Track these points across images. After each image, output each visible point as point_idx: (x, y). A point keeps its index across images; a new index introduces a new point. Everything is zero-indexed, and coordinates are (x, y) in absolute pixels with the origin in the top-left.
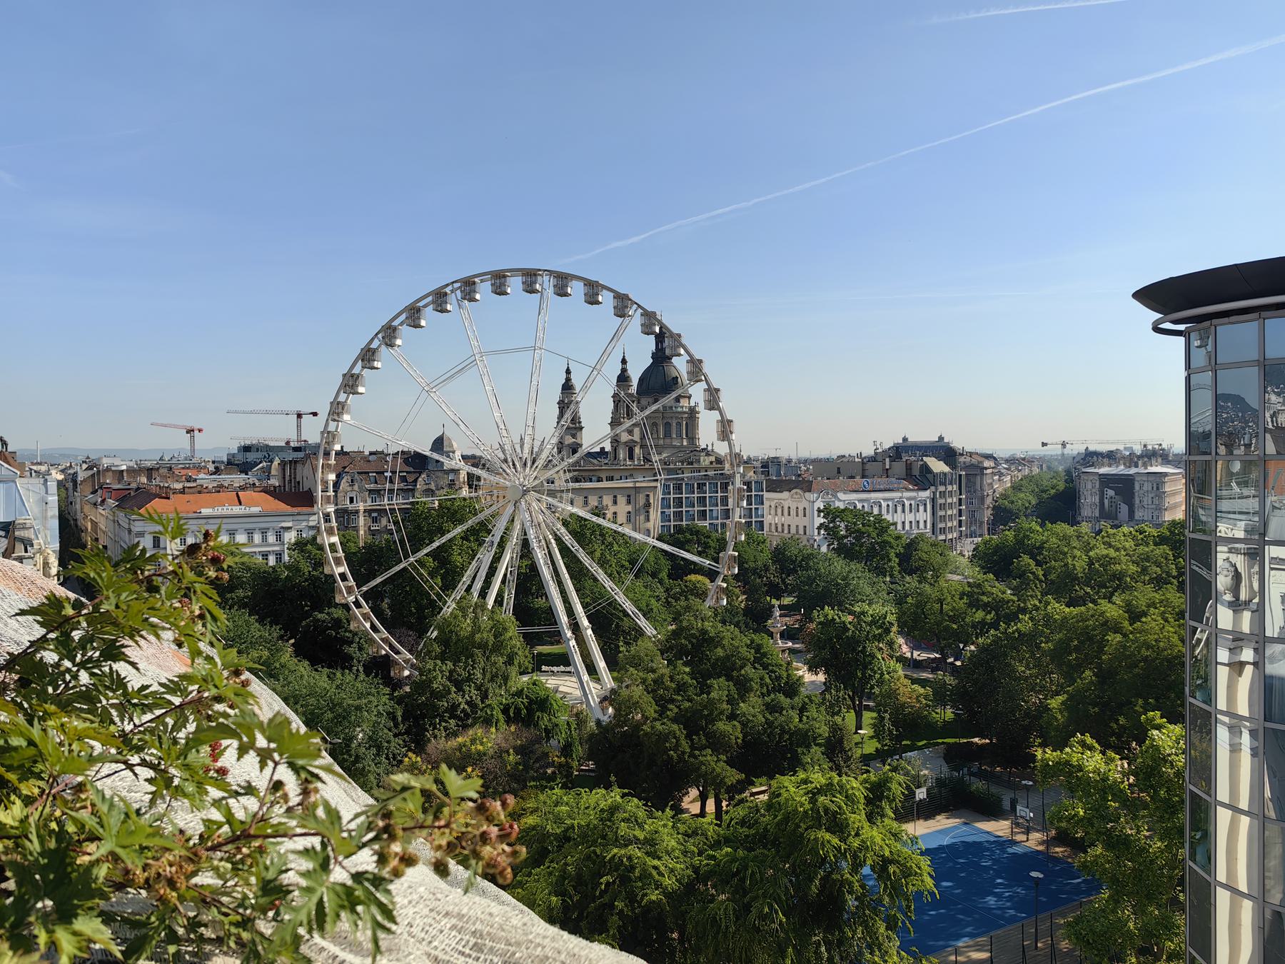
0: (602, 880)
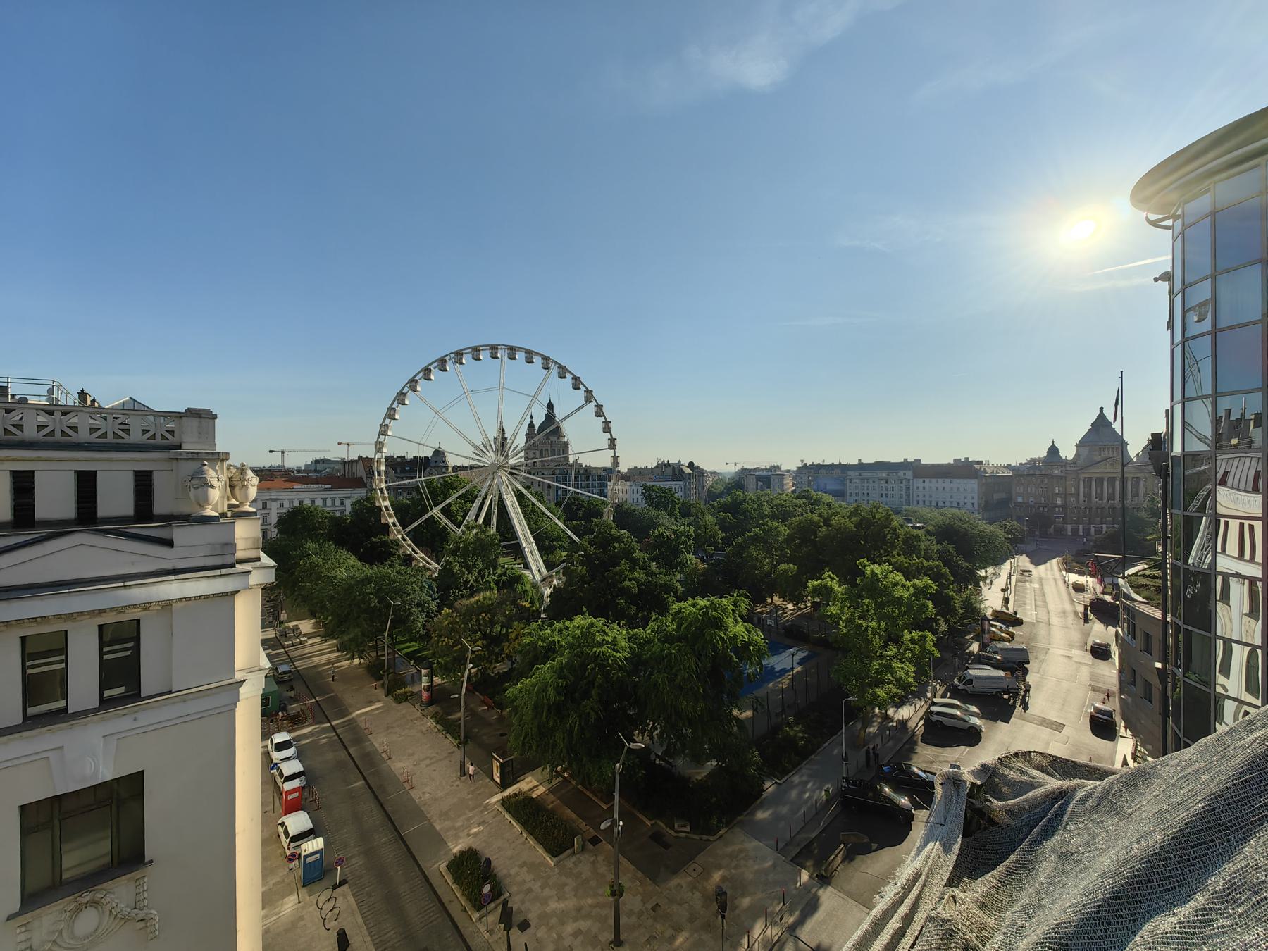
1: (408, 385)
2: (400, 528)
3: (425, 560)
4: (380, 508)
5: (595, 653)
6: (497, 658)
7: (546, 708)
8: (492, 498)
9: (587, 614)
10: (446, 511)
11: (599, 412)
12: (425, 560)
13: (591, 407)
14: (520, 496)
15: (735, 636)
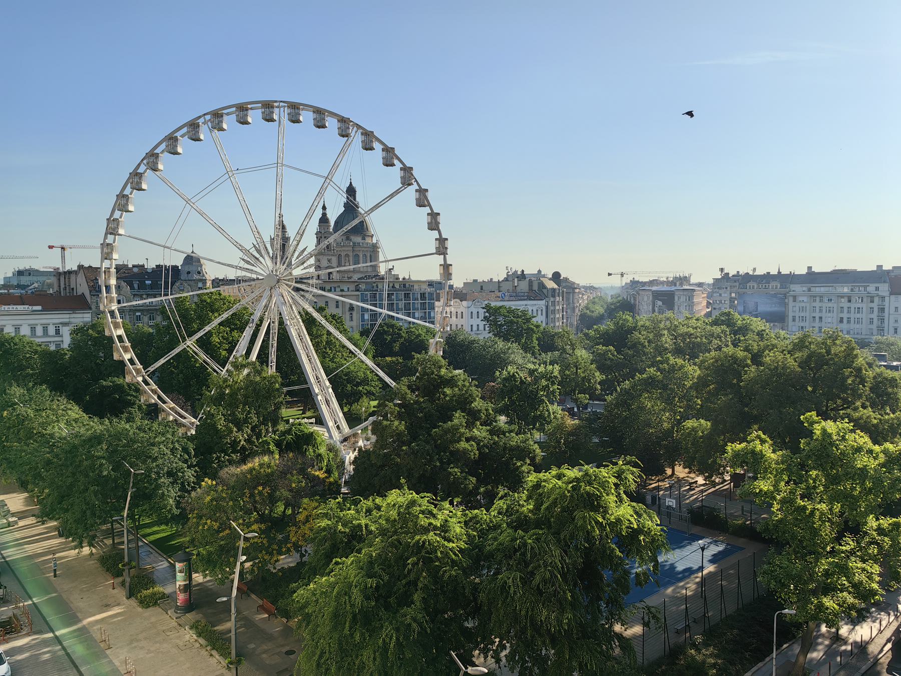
0: (409, 562)
1: (145, 162)
2: (140, 366)
3: (177, 412)
4: (110, 339)
5: (418, 541)
6: (280, 548)
7: (350, 616)
8: (269, 324)
9: (406, 488)
10: (204, 343)
11: (422, 200)
12: (177, 412)
13: (410, 193)
14: (309, 322)
15: (619, 521)
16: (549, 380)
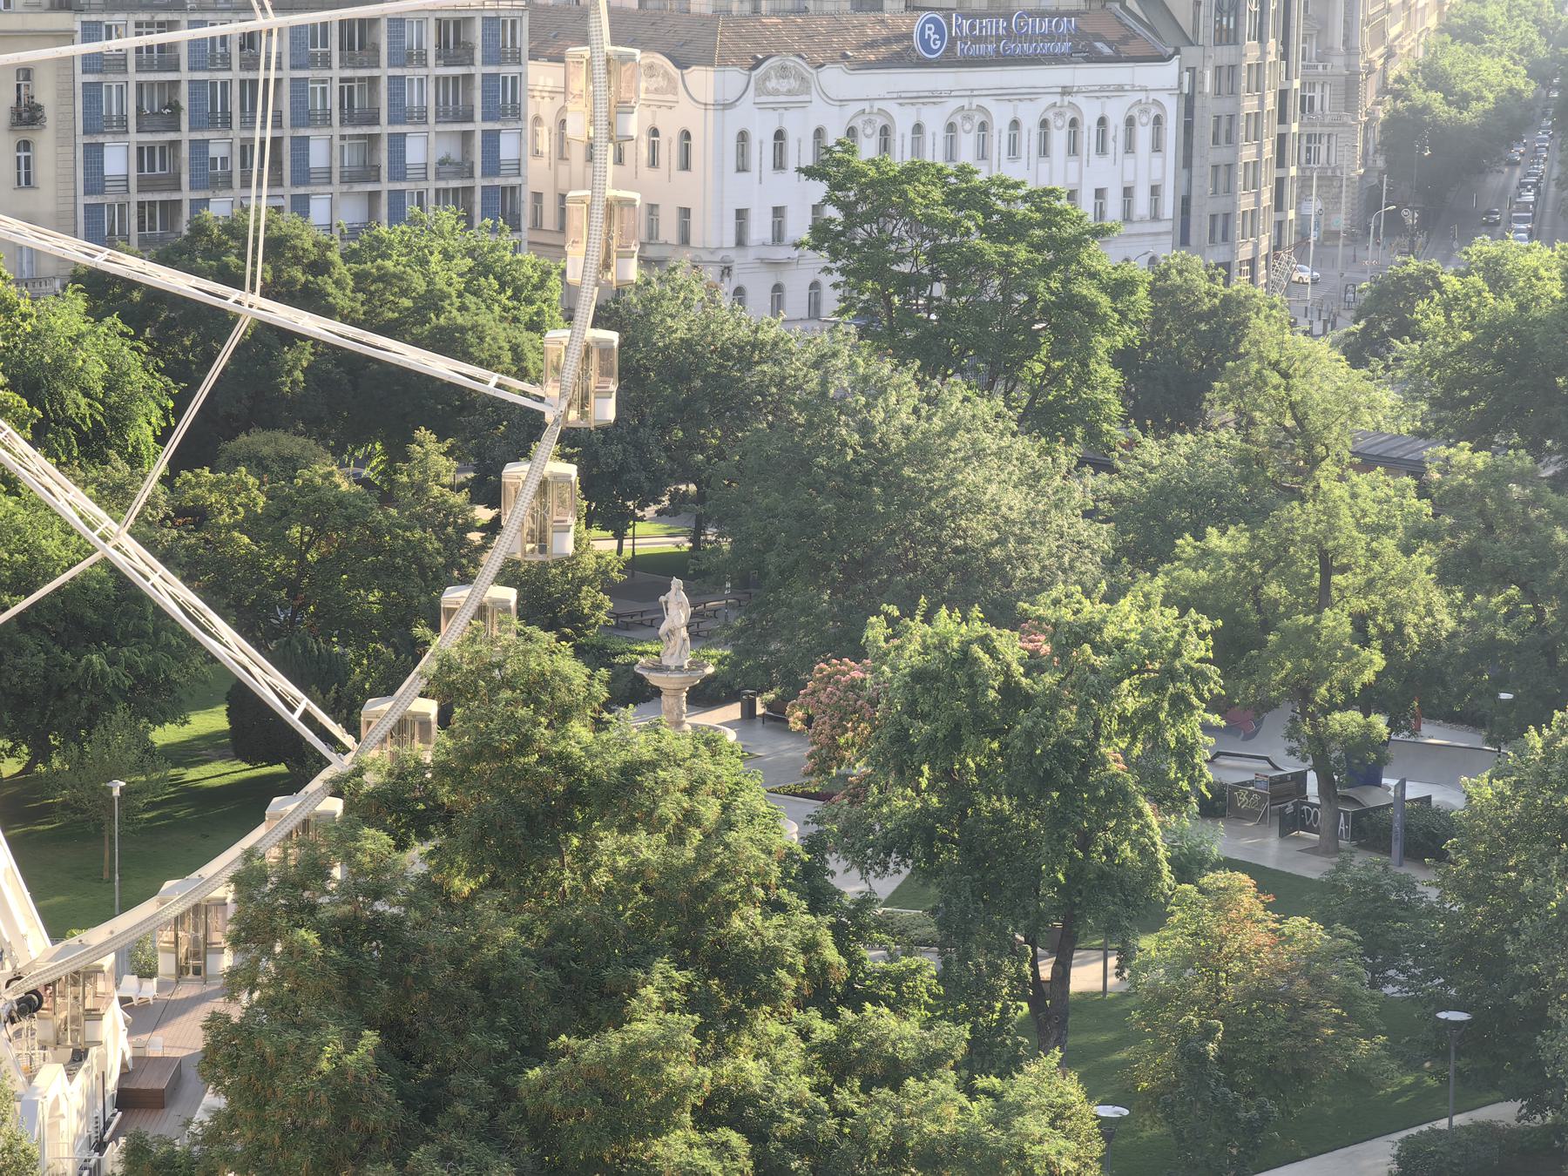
16: (1160, 688)
